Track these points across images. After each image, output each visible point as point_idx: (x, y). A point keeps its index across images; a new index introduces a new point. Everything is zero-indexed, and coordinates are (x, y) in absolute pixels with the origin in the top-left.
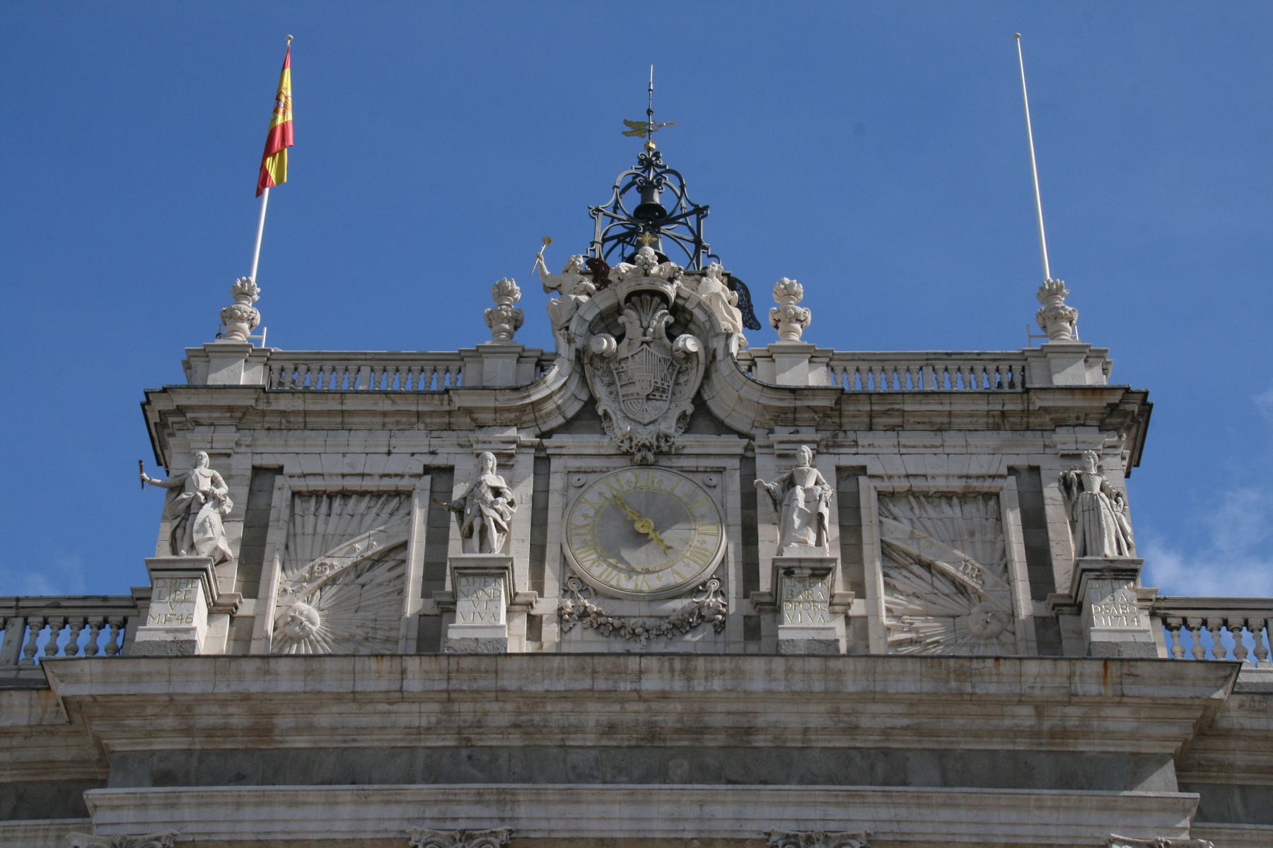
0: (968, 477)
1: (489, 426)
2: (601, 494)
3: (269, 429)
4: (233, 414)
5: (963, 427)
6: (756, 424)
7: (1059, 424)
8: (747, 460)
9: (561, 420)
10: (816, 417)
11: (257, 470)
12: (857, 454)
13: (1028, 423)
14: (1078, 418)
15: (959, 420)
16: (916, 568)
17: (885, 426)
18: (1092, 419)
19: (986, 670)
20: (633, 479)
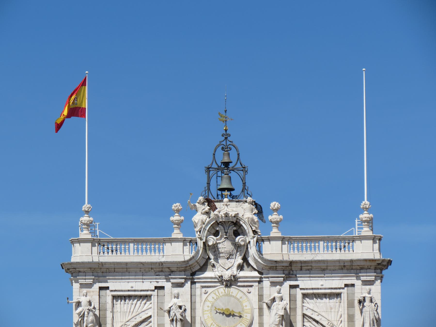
0: (332, 288)
1: (175, 272)
2: (213, 298)
3: (103, 272)
4: (91, 269)
5: (331, 269)
6: (263, 268)
7: (362, 269)
8: (260, 282)
9: (199, 267)
10: (283, 268)
11: (101, 288)
13: (352, 268)
14: (368, 267)
15: (330, 267)
16: (314, 322)
18: (372, 267)
20: (223, 292)
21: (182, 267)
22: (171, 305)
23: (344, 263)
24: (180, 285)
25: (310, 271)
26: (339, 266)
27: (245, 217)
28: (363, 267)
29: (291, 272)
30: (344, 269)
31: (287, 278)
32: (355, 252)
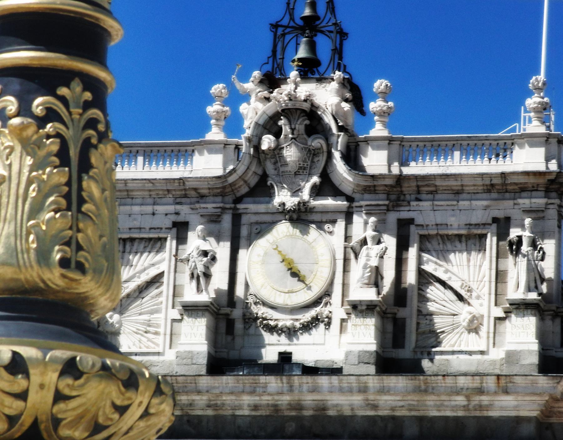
1: (207, 196)
6: (355, 191)
10: (387, 189)
12: (410, 210)
14: (533, 187)
15: (467, 188)
17: (427, 191)
18: (541, 187)
19: (439, 381)
21: (216, 188)
22: (192, 251)
23: (491, 180)
24: (214, 219)
25: (434, 196)
26: (483, 185)
27: (329, 104)
28: (526, 187)
29: (402, 197)
30: (493, 191)
31: (393, 206)
32: (514, 162)
